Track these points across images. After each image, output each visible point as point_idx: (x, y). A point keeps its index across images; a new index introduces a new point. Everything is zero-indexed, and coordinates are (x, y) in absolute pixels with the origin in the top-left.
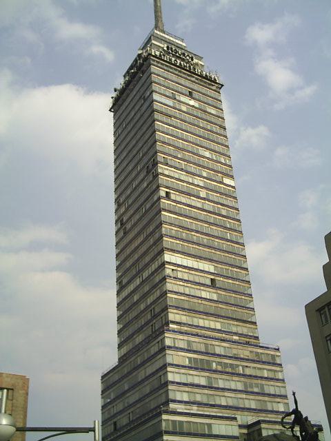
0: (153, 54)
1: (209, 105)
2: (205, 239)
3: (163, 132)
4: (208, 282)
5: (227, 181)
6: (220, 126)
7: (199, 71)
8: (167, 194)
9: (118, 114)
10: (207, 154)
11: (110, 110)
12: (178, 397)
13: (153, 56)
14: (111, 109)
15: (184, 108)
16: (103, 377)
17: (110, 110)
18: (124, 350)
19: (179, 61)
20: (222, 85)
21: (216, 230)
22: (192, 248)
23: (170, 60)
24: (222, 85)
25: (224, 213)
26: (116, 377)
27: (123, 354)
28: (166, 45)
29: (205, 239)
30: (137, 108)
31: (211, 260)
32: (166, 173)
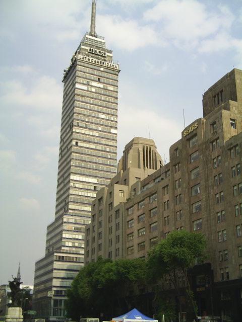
0: (79, 58)
1: (109, 84)
2: (94, 166)
3: (79, 107)
4: (93, 188)
5: (113, 131)
6: (114, 97)
8: (77, 143)
10: (103, 116)
12: (67, 244)
15: (93, 90)
16: (48, 227)
21: (101, 160)
22: (86, 171)
25: (108, 150)
29: (94, 166)
31: (96, 177)
32: (77, 131)
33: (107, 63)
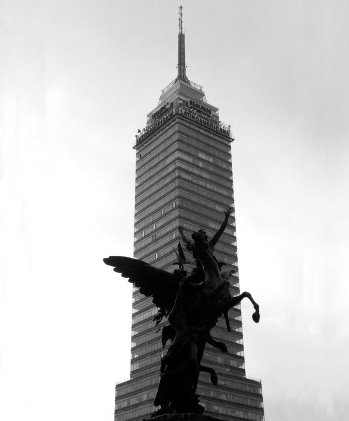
7: (216, 126)
9: (143, 153)
11: (134, 148)
13: (179, 114)
14: (136, 146)
15: (201, 164)
17: (134, 148)
18: (137, 366)
19: (199, 118)
20: (233, 140)
23: (193, 117)
24: (233, 140)
26: (129, 389)
27: (135, 369)
28: (189, 100)
30: (161, 157)
33: (216, 126)
